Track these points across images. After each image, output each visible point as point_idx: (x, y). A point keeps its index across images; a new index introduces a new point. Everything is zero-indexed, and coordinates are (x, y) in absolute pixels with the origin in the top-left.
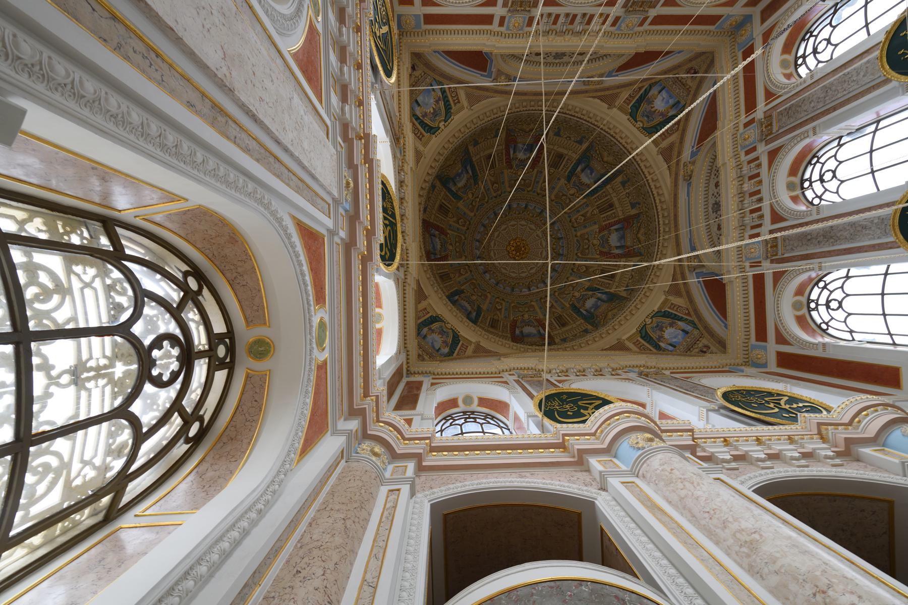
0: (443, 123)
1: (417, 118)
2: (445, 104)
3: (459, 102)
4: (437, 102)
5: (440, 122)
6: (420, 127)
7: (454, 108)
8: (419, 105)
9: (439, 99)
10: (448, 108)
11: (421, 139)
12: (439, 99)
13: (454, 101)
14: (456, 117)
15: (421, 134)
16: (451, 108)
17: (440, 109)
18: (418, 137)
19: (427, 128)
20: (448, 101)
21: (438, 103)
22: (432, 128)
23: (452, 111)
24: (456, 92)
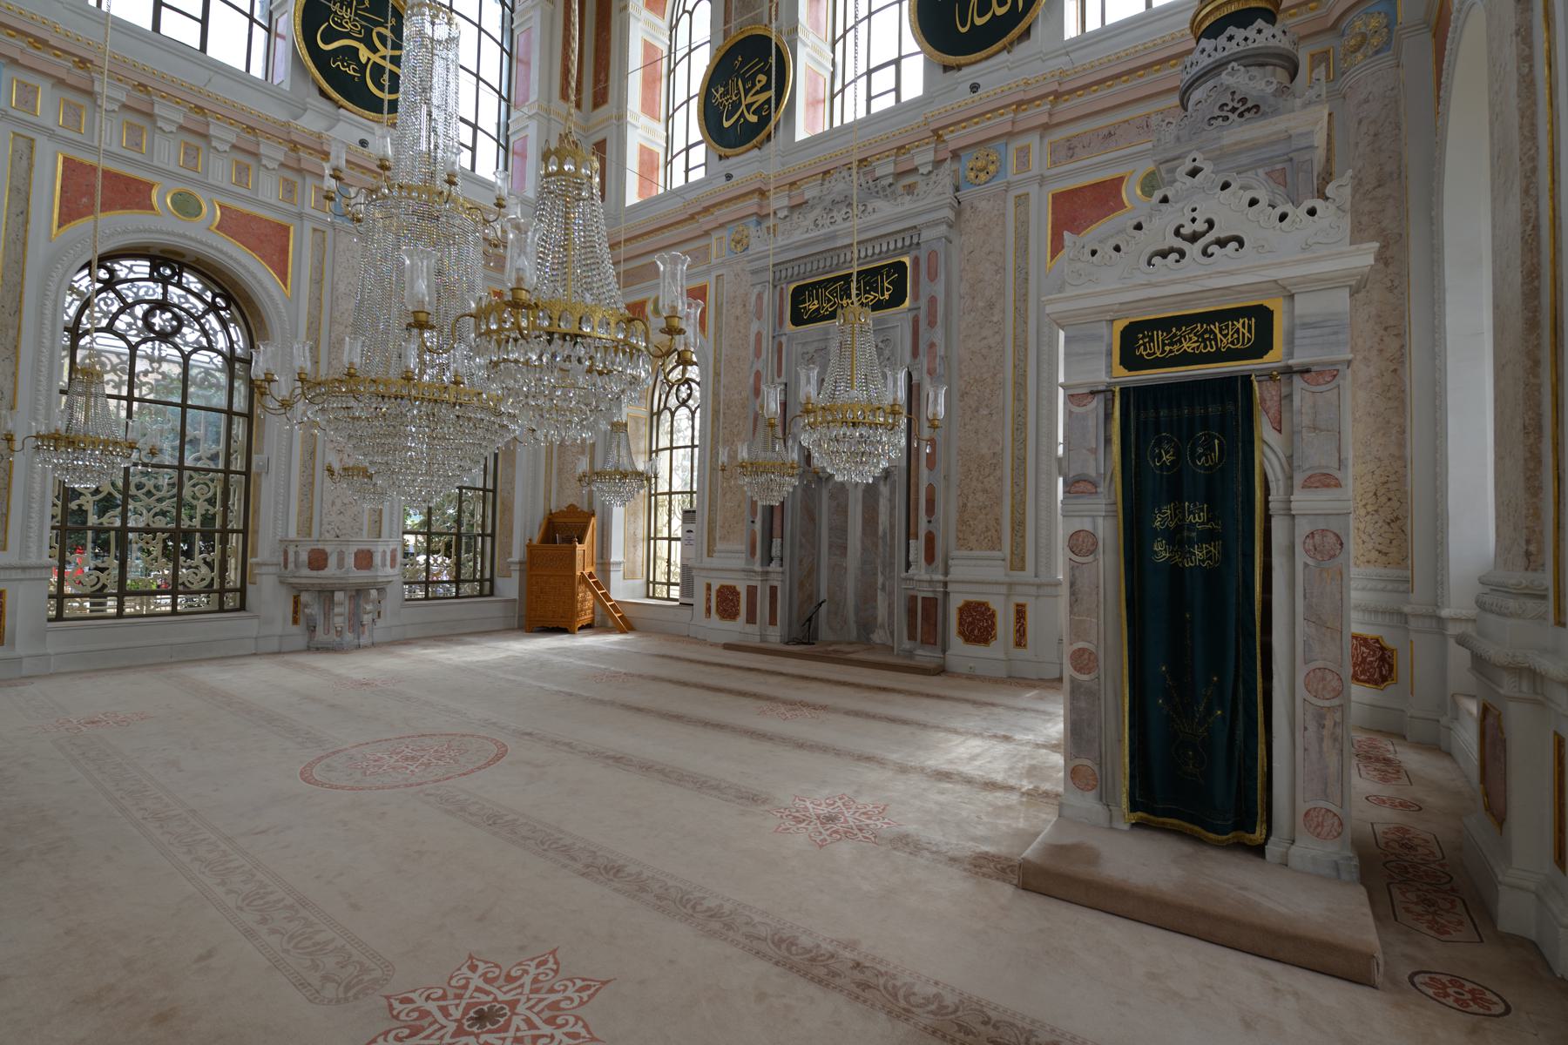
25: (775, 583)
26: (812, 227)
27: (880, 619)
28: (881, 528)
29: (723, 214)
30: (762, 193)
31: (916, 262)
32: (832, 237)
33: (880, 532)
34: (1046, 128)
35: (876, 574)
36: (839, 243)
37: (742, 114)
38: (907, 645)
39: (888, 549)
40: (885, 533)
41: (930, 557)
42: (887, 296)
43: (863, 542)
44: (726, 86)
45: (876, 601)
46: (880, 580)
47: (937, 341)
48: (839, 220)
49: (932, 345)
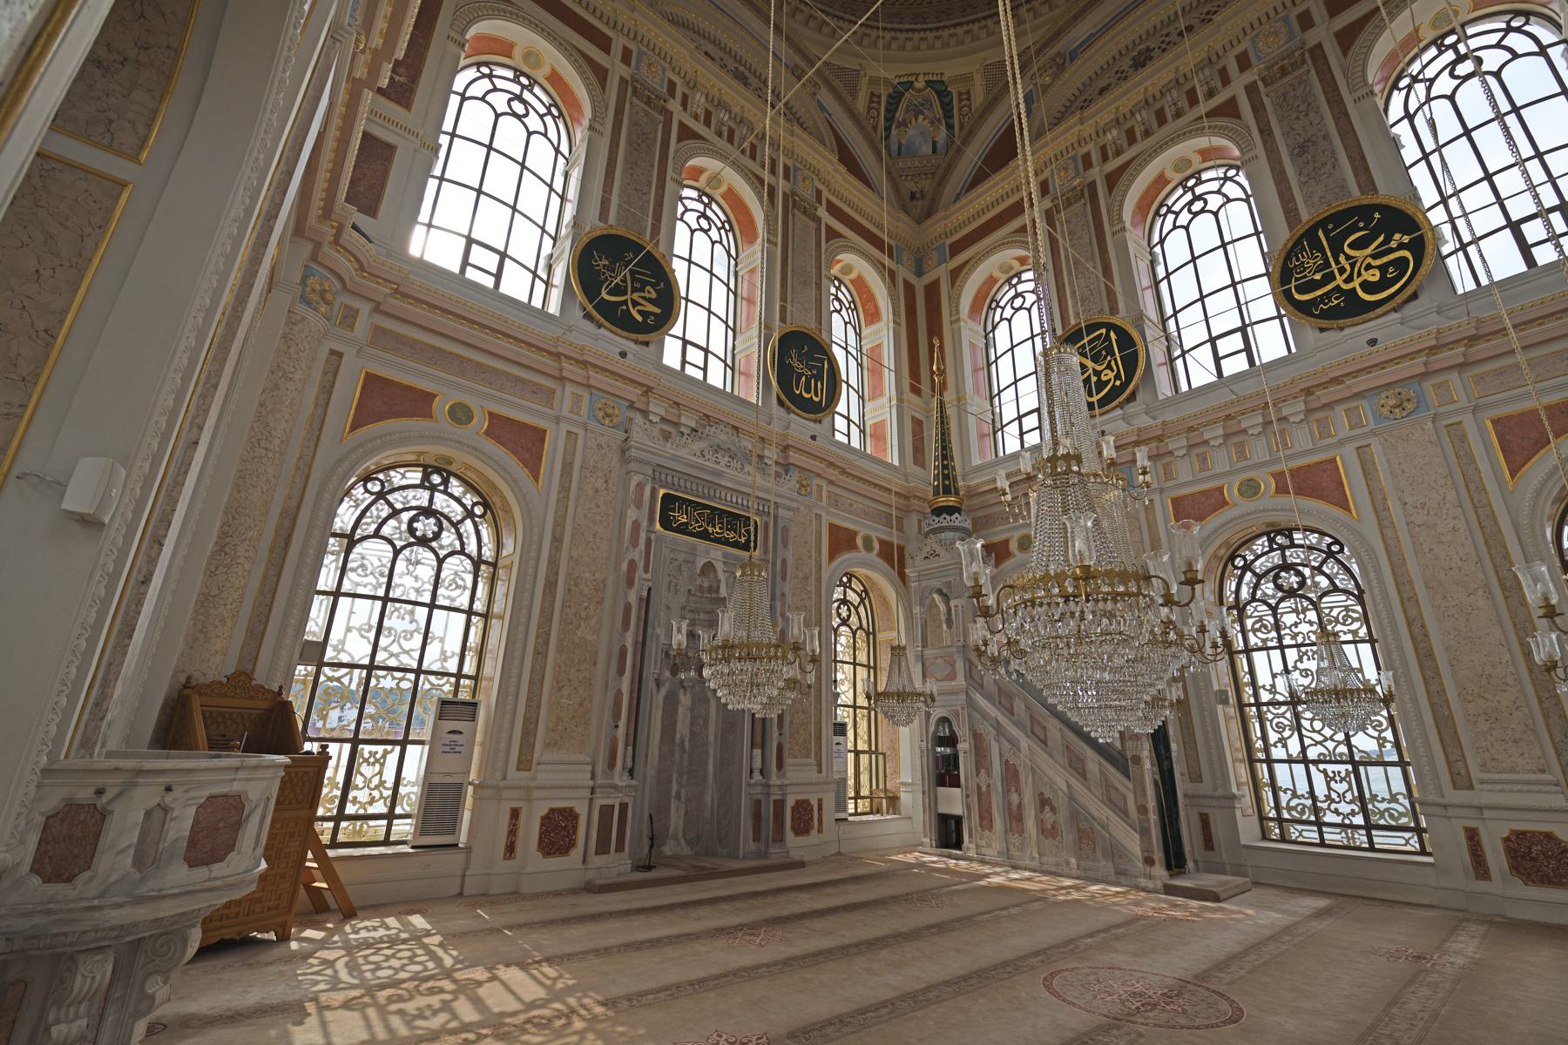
0: (916, 84)
1: (950, 127)
2: (896, 110)
3: (872, 95)
4: (904, 124)
5: (920, 90)
6: (956, 111)
7: (884, 92)
8: (934, 143)
9: (900, 125)
10: (895, 99)
11: (968, 92)
12: (900, 125)
13: (879, 103)
14: (890, 76)
15: (961, 100)
16: (889, 96)
17: (907, 110)
18: (968, 99)
19: (946, 100)
20: (887, 110)
21: (904, 120)
22: (940, 94)
23: (891, 90)
24: (870, 109)
25: (626, 800)
26: (698, 454)
27: (672, 829)
28: (678, 735)
29: (597, 378)
30: (648, 390)
31: (766, 525)
32: (719, 474)
33: (677, 740)
34: (831, 482)
35: (670, 782)
36: (723, 483)
37: (625, 302)
38: (752, 846)
39: (686, 756)
40: (683, 741)
41: (780, 765)
42: (743, 540)
43: (660, 749)
44: (613, 263)
45: (669, 810)
46: (675, 787)
47: (787, 592)
48: (723, 463)
49: (783, 595)
